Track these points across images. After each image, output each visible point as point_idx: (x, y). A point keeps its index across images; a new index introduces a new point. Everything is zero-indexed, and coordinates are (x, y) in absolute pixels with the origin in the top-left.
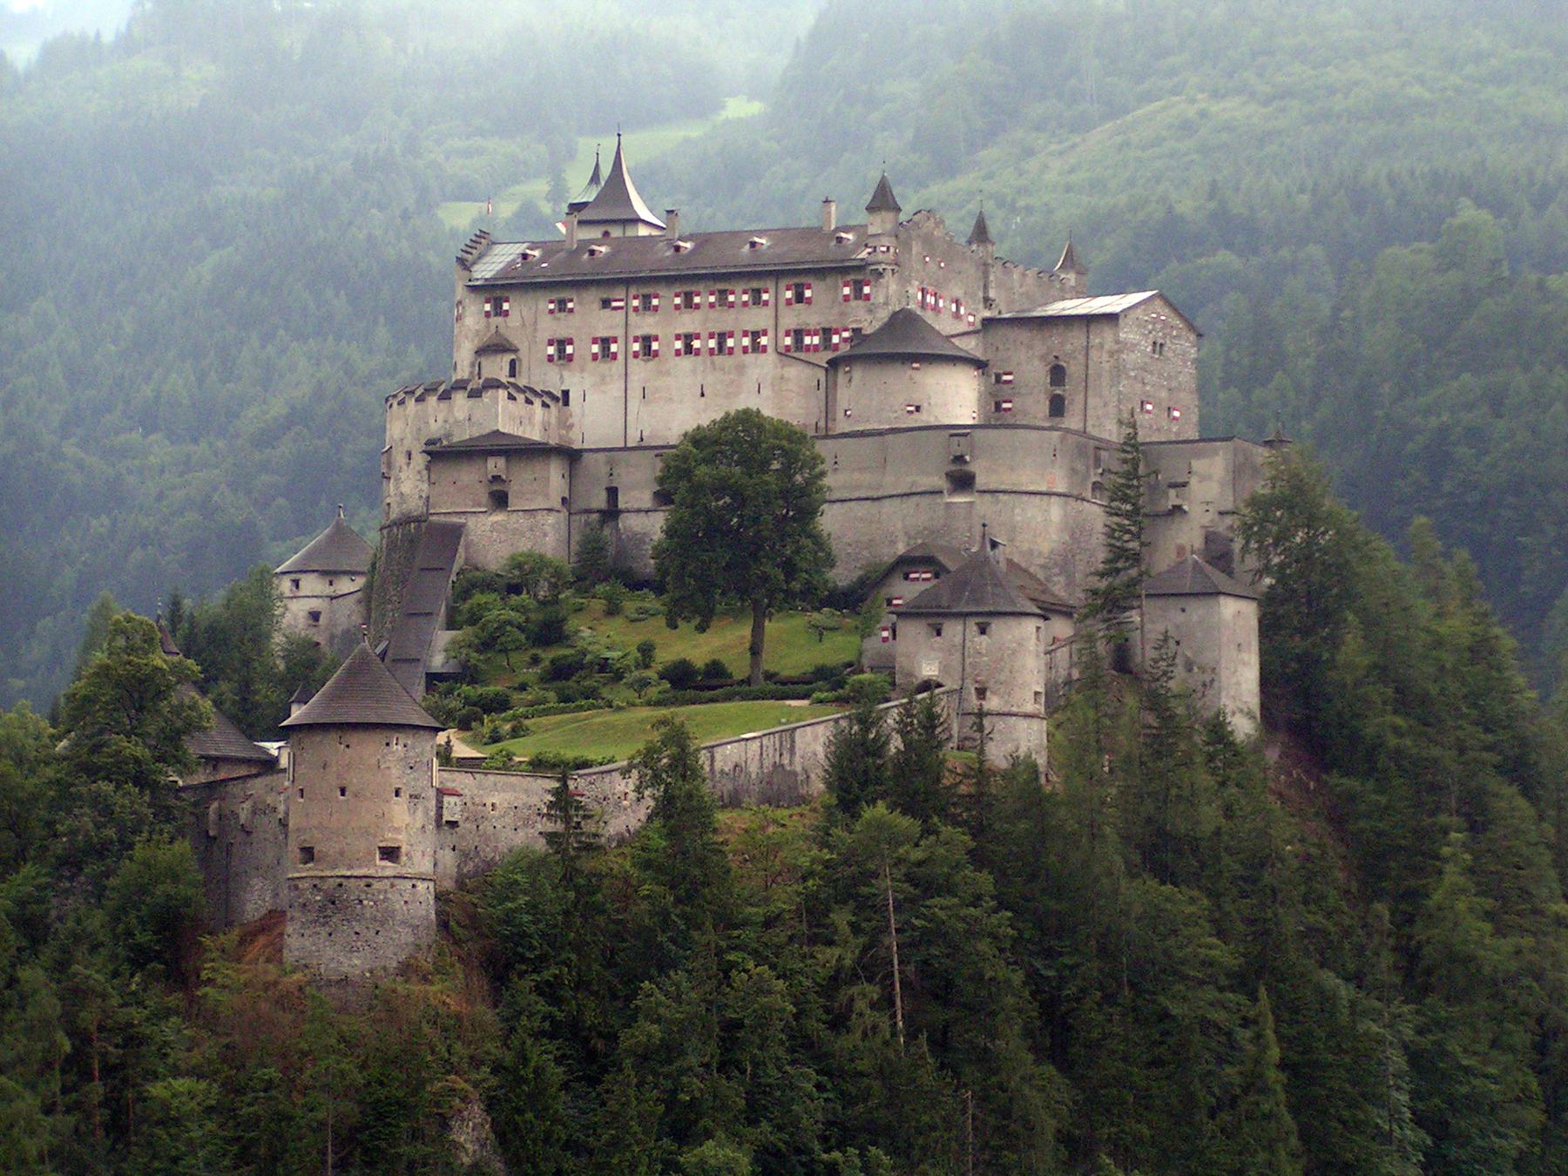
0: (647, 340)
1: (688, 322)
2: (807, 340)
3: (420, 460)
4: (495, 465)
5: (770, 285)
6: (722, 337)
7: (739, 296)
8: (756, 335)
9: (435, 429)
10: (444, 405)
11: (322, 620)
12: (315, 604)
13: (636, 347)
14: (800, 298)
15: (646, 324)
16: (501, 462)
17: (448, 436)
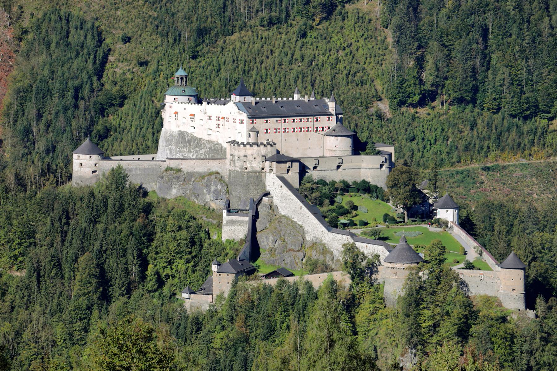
0: (285, 129)
1: (294, 125)
2: (319, 129)
3: (259, 159)
4: (289, 164)
5: (312, 117)
6: (301, 128)
7: (304, 119)
8: (308, 128)
9: (263, 153)
10: (265, 148)
11: (97, 165)
12: (96, 162)
13: (284, 130)
14: (317, 120)
15: (285, 126)
16: (290, 163)
17: (267, 155)
